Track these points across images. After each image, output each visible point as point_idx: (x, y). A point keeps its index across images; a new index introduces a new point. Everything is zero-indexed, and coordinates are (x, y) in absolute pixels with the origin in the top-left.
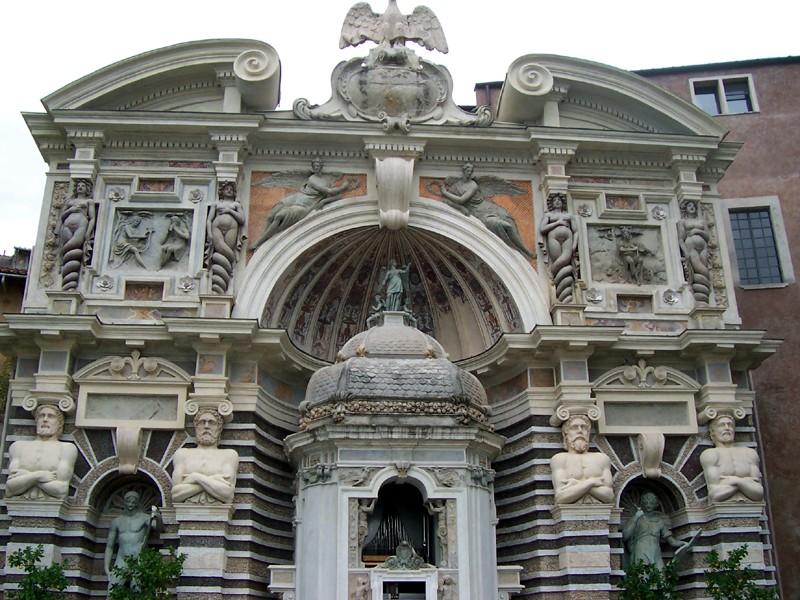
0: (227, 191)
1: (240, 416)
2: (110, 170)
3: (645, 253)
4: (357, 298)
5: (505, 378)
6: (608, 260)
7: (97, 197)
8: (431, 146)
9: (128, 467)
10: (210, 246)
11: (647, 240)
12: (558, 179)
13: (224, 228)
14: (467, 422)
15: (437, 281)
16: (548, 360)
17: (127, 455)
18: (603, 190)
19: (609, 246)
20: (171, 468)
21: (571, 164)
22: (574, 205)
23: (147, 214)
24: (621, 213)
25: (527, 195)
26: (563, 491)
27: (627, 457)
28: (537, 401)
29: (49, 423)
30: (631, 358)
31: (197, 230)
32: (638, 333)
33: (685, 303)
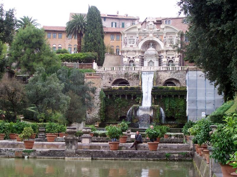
0: (137, 38)
1: (139, 56)
2: (128, 36)
3: (173, 41)
4: (149, 44)
5: (160, 52)
6: (169, 42)
8: (154, 33)
9: (131, 60)
11: (173, 40)
12: (165, 35)
14: (156, 56)
16: (163, 51)
18: (169, 36)
19: (169, 41)
21: (166, 34)
23: (131, 39)
24: (171, 38)
25: (163, 36)
26: (163, 61)
29: (125, 57)
30: (170, 51)
31: (135, 41)
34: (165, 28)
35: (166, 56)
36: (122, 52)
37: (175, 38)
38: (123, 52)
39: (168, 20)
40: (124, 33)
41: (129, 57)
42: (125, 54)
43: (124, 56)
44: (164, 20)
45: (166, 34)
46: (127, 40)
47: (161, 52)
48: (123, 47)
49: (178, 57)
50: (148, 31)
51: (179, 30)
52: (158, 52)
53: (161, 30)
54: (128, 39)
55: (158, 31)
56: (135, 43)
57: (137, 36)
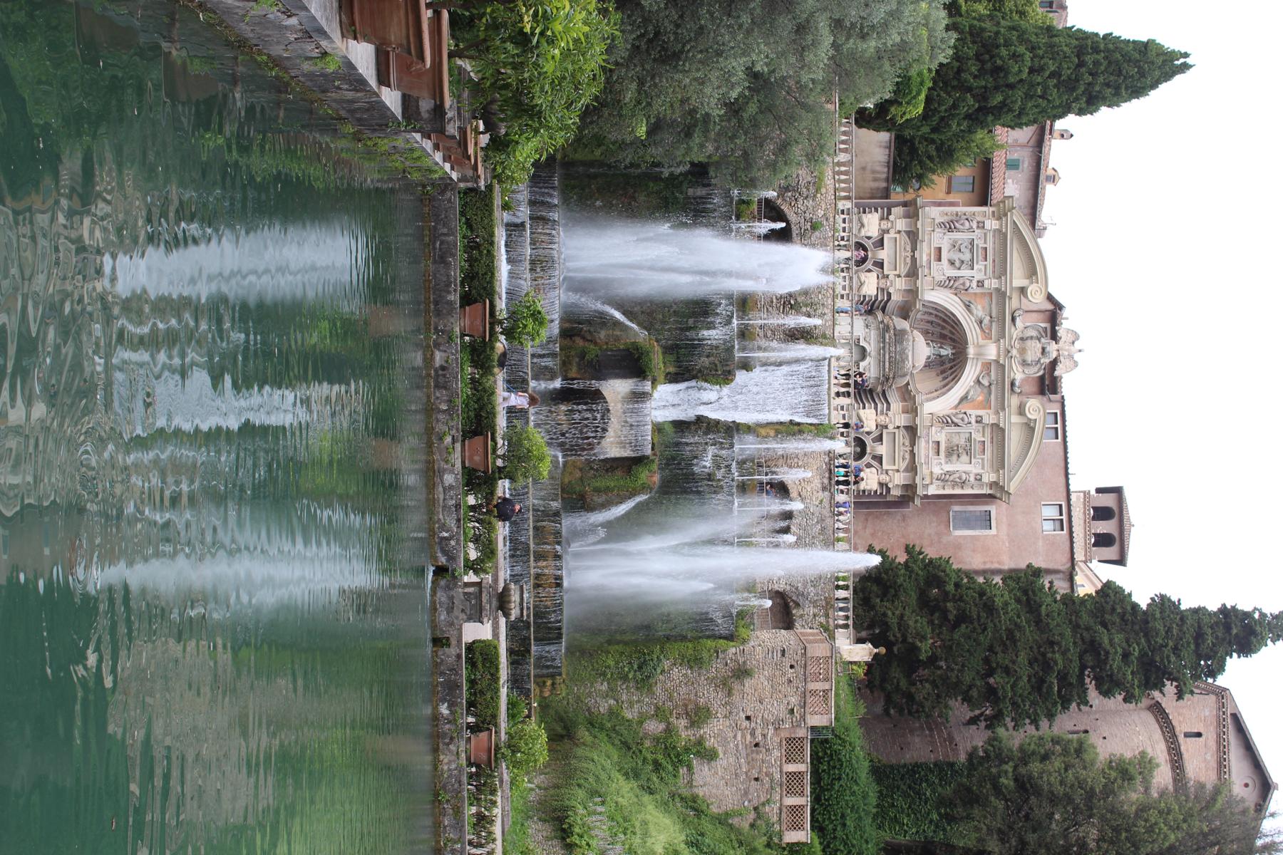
0: (980, 284)
1: (889, 295)
2: (990, 237)
4: (943, 336)
5: (907, 395)
6: (955, 441)
7: (977, 231)
8: (1003, 366)
10: (956, 279)
11: (964, 458)
12: (989, 417)
13: (964, 284)
15: (948, 368)
17: (874, 254)
18: (987, 439)
20: (869, 271)
21: (997, 425)
22: (980, 427)
26: (862, 412)
27: (874, 440)
28: (896, 405)
29: (885, 225)
30: (913, 444)
31: (965, 272)
32: (923, 448)
33: (937, 471)
34: (1023, 420)
35: (886, 427)
36: (911, 209)
37: (974, 469)
38: (912, 210)
39: (1059, 426)
40: (1006, 215)
41: (882, 240)
42: (901, 224)
43: (891, 217)
44: (1059, 405)
45: (997, 425)
46: (971, 230)
47: (904, 400)
48: (935, 213)
49: (881, 484)
50: (1011, 338)
51: (1012, 487)
52: (908, 384)
53: (1014, 401)
54: (971, 236)
55: (1013, 384)
56: (953, 273)
57: (986, 285)
